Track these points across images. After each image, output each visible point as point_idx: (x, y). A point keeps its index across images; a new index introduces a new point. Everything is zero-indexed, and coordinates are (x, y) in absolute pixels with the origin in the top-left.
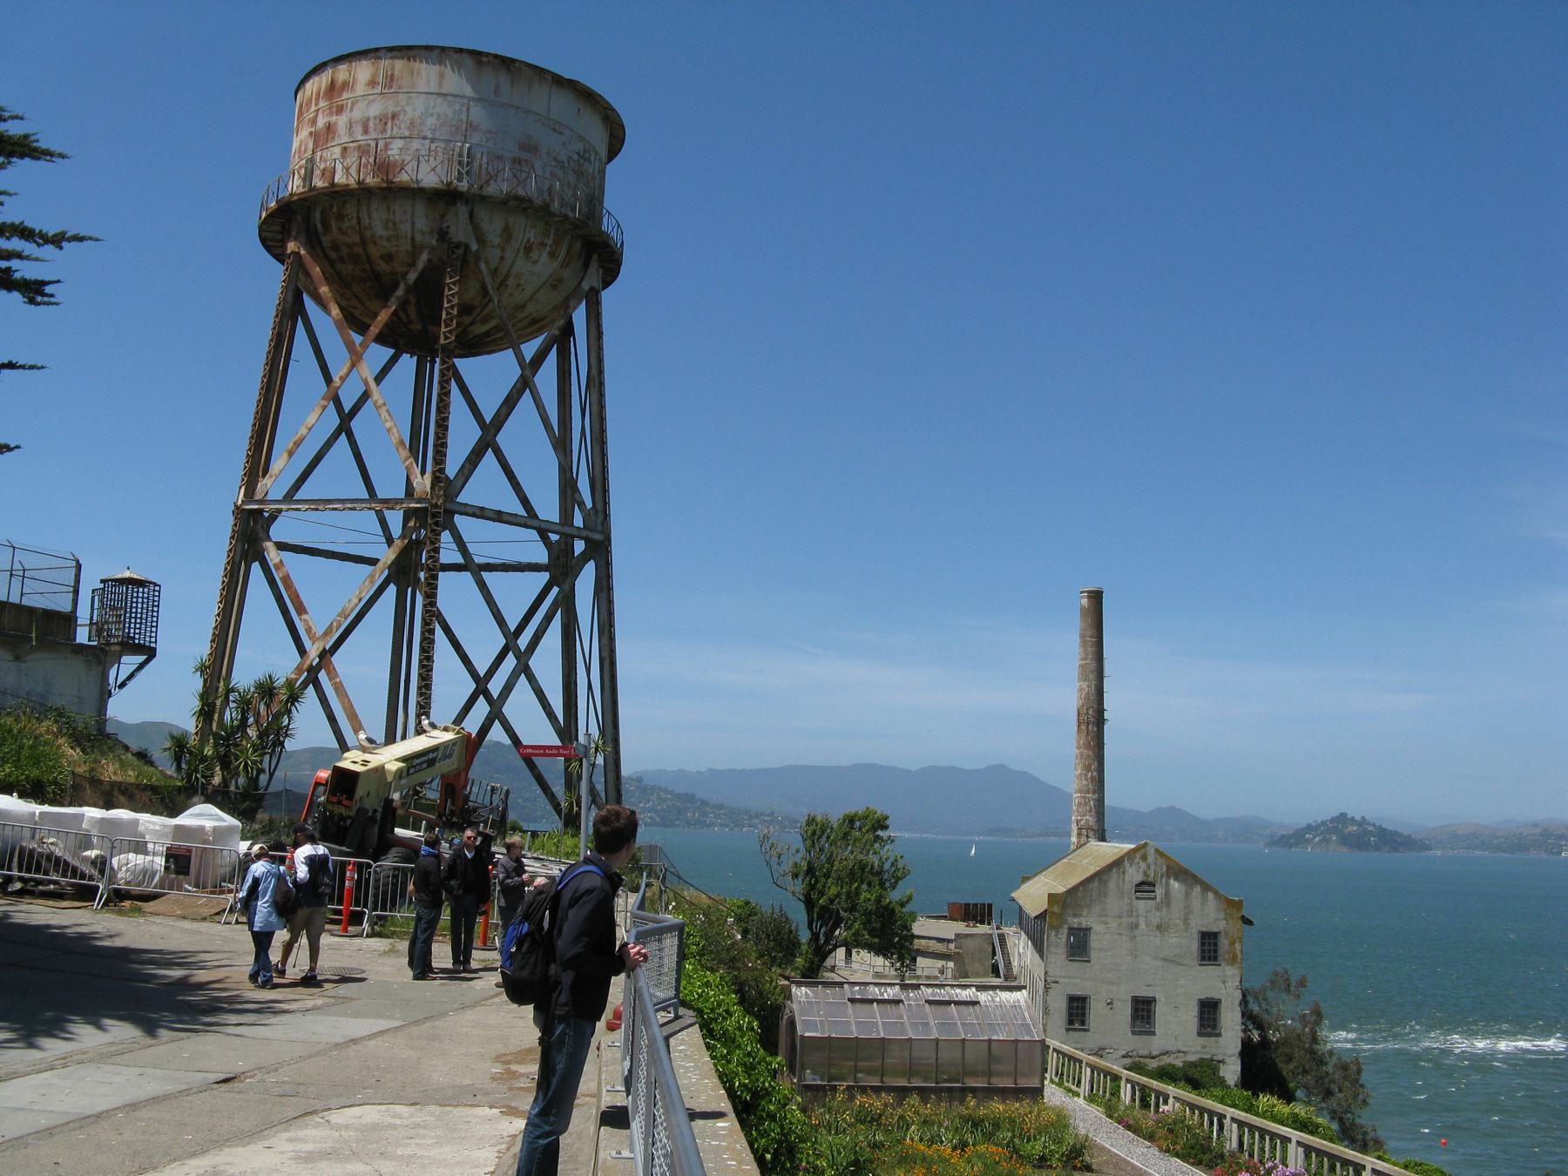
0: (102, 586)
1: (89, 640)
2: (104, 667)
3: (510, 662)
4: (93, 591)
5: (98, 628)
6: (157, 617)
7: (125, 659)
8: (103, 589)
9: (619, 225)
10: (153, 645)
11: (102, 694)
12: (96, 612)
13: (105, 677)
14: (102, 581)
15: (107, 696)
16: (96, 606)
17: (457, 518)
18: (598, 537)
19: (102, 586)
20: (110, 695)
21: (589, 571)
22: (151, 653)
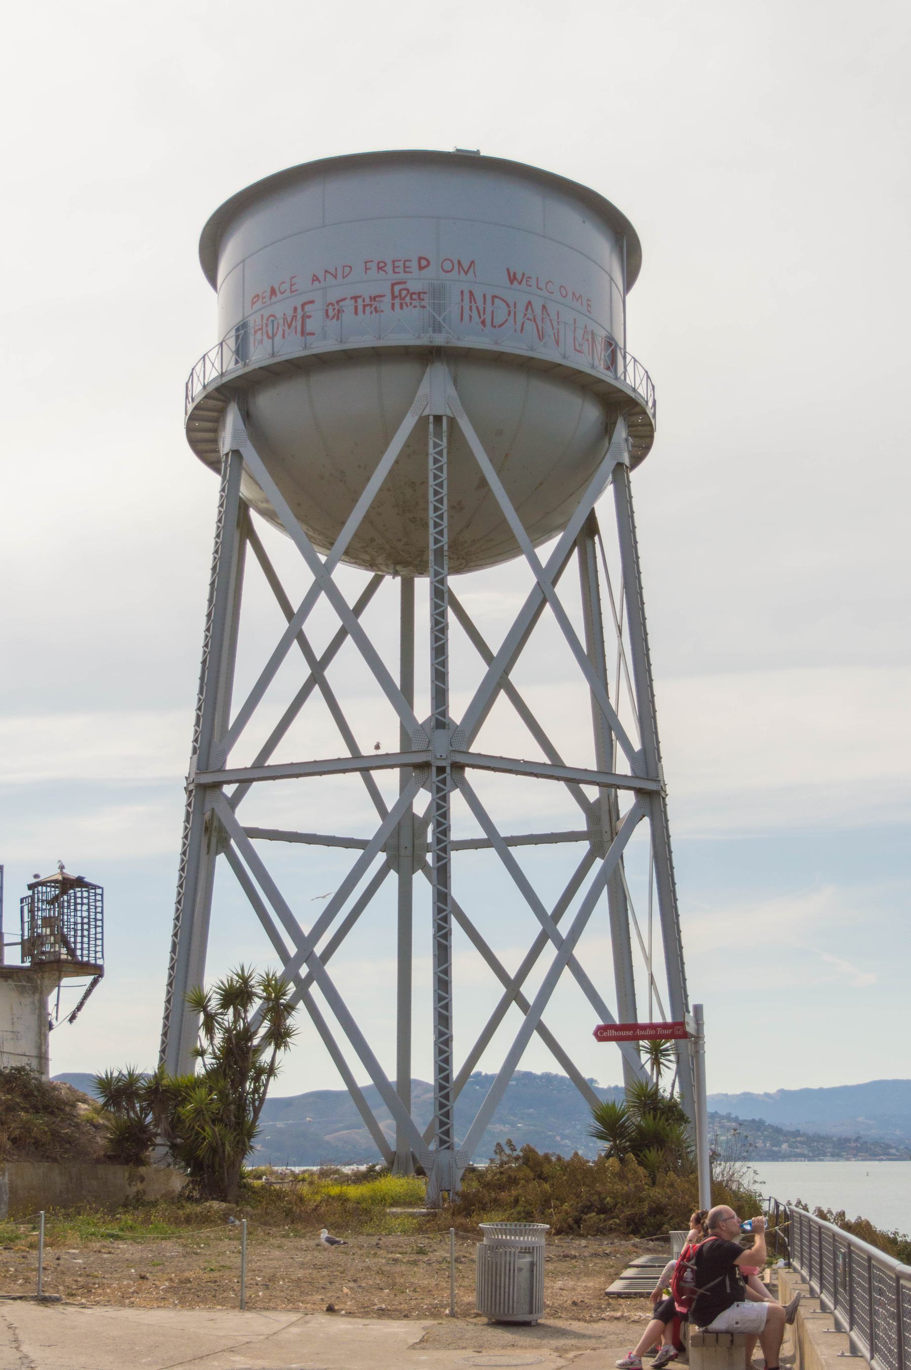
0: (30, 893)
1: (23, 962)
2: (41, 993)
3: (550, 952)
4: (22, 901)
5: (30, 946)
6: (102, 927)
7: (65, 981)
8: (32, 897)
9: (648, 377)
10: (99, 962)
11: (40, 1027)
12: (26, 925)
13: (43, 1005)
14: (31, 887)
15: (48, 1027)
16: (26, 919)
17: (470, 774)
18: (650, 786)
19: (30, 893)
20: (51, 1027)
21: (643, 829)
22: (97, 971)
